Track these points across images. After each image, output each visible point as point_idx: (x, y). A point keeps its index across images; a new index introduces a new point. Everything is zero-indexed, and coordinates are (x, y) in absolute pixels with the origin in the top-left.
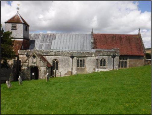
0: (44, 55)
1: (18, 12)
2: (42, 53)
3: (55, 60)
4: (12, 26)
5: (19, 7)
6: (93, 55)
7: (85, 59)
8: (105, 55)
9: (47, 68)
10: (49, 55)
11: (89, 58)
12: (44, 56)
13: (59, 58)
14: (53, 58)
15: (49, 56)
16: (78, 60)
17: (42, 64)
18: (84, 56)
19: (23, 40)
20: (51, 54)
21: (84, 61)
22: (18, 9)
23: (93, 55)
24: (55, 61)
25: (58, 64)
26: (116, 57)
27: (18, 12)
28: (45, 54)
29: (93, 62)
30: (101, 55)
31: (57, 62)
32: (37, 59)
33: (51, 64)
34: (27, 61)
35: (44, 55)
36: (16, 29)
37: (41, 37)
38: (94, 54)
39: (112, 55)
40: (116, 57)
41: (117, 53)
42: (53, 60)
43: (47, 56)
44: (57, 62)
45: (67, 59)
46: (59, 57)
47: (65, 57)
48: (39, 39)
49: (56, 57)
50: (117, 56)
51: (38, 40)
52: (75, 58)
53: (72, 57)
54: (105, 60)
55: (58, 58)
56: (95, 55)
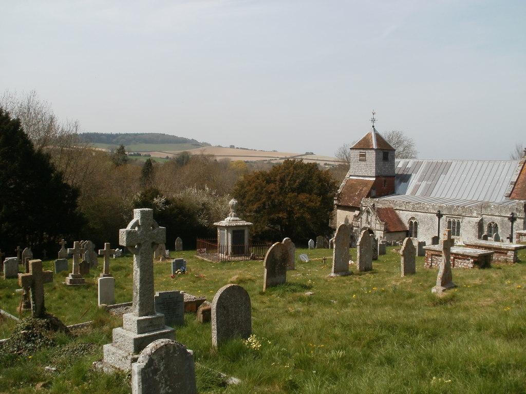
3: (413, 218)
4: (361, 155)
6: (475, 215)
7: (460, 220)
11: (467, 219)
13: (420, 216)
14: (411, 214)
16: (449, 222)
17: (378, 226)
19: (374, 179)
21: (459, 223)
23: (475, 215)
24: (412, 221)
25: (418, 226)
26: (518, 220)
27: (373, 126)
28: (398, 208)
29: (474, 227)
31: (416, 223)
33: (407, 226)
36: (365, 160)
39: (508, 215)
42: (410, 219)
44: (416, 223)
50: (521, 218)
52: (444, 217)
53: (440, 216)
54: (497, 225)
55: (418, 215)
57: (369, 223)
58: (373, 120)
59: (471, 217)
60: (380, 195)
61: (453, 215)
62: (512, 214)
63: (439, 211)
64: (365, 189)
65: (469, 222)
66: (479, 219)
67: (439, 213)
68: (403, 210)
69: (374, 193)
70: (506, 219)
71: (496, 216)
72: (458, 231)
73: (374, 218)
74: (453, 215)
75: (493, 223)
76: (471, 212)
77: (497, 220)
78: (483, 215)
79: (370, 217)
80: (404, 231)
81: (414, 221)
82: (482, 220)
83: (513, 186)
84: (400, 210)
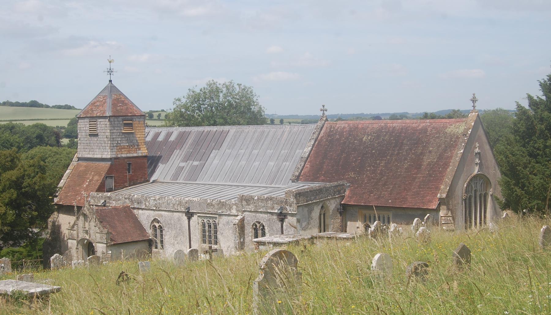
0: (134, 208)
1: (110, 81)
2: (132, 201)
3: (155, 220)
5: (113, 66)
7: (217, 221)
8: (261, 210)
9: (107, 246)
10: (144, 207)
11: (224, 219)
12: (135, 211)
14: (152, 214)
15: (144, 211)
16: (204, 225)
18: (211, 214)
20: (147, 204)
21: (216, 227)
22: (110, 72)
27: (110, 81)
28: (136, 205)
30: (250, 211)
31: (160, 227)
32: (90, 222)
33: (150, 231)
34: (76, 227)
35: (134, 208)
37: (190, 141)
38: (234, 207)
40: (289, 218)
41: (290, 206)
42: (152, 222)
43: (140, 211)
44: (160, 226)
45: (179, 219)
46: (163, 213)
47: (175, 214)
48: (182, 149)
49: (157, 212)
50: (292, 215)
51: (181, 152)
52: (195, 218)
53: (189, 215)
55: (162, 216)
56: (238, 211)
57: (87, 232)
58: (110, 72)
59: (229, 215)
60: (120, 185)
61: (206, 213)
62: (282, 208)
63: (189, 208)
64: (96, 178)
65: (228, 223)
66: (239, 218)
67: (188, 212)
68: (143, 209)
69: (111, 183)
70: (275, 217)
71: (261, 212)
72: (216, 237)
73: (93, 224)
74: (206, 213)
75: (259, 223)
76: (230, 208)
77: (263, 218)
78: (244, 211)
79: (87, 224)
80: (145, 241)
81: (157, 225)
82: (242, 220)
83: (303, 164)
84: (138, 209)
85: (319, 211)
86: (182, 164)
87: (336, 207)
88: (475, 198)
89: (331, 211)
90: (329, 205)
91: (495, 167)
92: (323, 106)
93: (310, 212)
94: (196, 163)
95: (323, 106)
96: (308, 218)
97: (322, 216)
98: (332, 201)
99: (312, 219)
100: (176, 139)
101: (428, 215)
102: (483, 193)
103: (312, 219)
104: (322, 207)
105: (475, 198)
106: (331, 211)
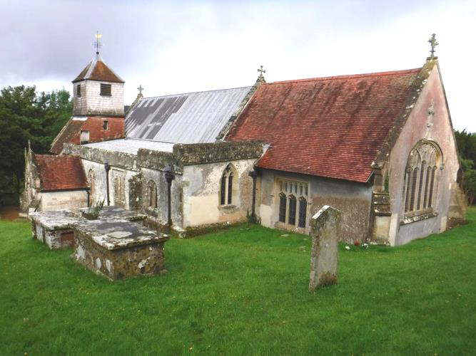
55: (93, 167)
85: (221, 173)
86: (150, 125)
87: (247, 170)
88: (422, 171)
89: (240, 175)
90: (236, 167)
91: (449, 136)
92: (262, 67)
93: (206, 174)
94: (158, 124)
95: (262, 67)
96: (203, 181)
97: (227, 180)
98: (243, 163)
99: (208, 182)
100: (154, 105)
101: (326, 207)
102: (432, 166)
103: (208, 182)
104: (228, 169)
105: (422, 171)
106: (240, 175)
